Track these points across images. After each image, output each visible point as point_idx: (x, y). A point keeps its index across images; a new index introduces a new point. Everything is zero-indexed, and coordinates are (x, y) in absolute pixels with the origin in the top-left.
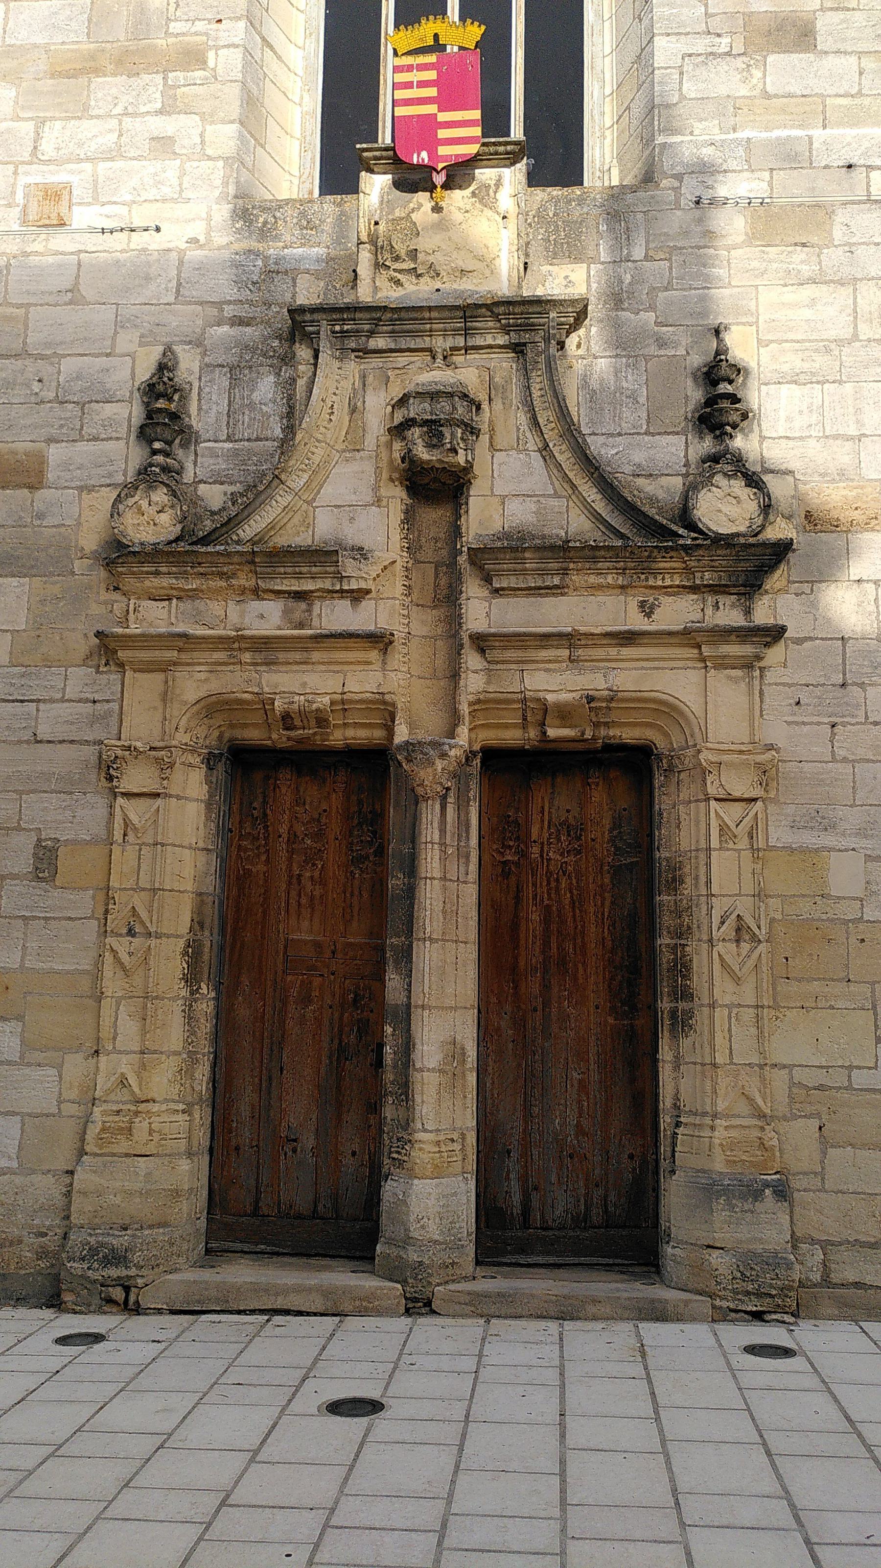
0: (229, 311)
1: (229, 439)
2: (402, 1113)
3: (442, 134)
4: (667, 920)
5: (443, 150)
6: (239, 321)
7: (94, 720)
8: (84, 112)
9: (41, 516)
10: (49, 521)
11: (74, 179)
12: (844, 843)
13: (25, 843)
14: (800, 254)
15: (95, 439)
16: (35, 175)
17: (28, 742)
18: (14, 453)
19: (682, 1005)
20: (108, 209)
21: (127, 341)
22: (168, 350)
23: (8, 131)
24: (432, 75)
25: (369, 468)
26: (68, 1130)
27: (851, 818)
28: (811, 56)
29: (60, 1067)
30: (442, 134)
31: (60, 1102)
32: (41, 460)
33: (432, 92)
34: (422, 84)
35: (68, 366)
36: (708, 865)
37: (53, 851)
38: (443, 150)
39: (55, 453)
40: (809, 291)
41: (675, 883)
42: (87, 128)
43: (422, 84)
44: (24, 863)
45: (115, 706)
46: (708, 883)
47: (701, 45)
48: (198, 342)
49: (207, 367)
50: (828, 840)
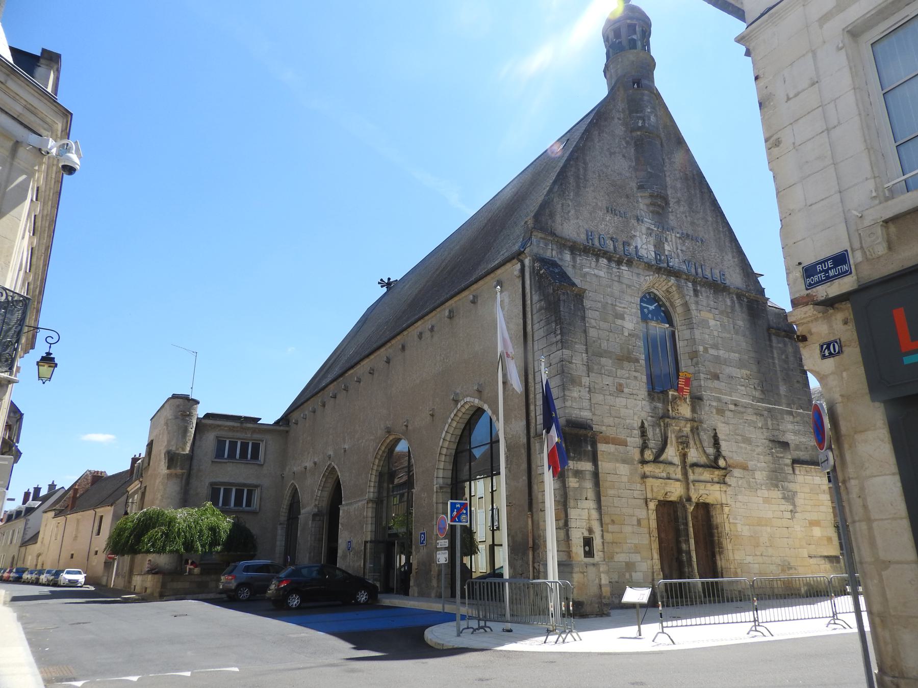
0: (650, 414)
1: (654, 440)
2: (690, 570)
3: (684, 390)
4: (716, 535)
5: (684, 393)
6: (652, 417)
7: (643, 494)
8: (622, 368)
9: (628, 452)
10: (630, 453)
11: (623, 382)
12: (739, 522)
13: (635, 518)
14: (722, 418)
15: (634, 437)
16: (617, 380)
17: (632, 498)
18: (622, 438)
19: (721, 550)
20: (629, 390)
21: (636, 418)
22: (642, 421)
23: (611, 370)
24: (684, 380)
25: (674, 449)
26: (650, 574)
27: (739, 518)
28: (718, 382)
29: (647, 562)
30: (684, 390)
31: (648, 569)
32: (627, 441)
33: (684, 383)
34: (683, 382)
35: (628, 421)
36: (725, 525)
37: (640, 520)
38: (684, 393)
39: (628, 439)
40: (724, 425)
41: (717, 528)
42: (624, 372)
43: (683, 382)
44: (635, 523)
45: (645, 492)
46: (725, 529)
47: (706, 376)
48: (646, 420)
49: (648, 425)
50: (737, 521)
